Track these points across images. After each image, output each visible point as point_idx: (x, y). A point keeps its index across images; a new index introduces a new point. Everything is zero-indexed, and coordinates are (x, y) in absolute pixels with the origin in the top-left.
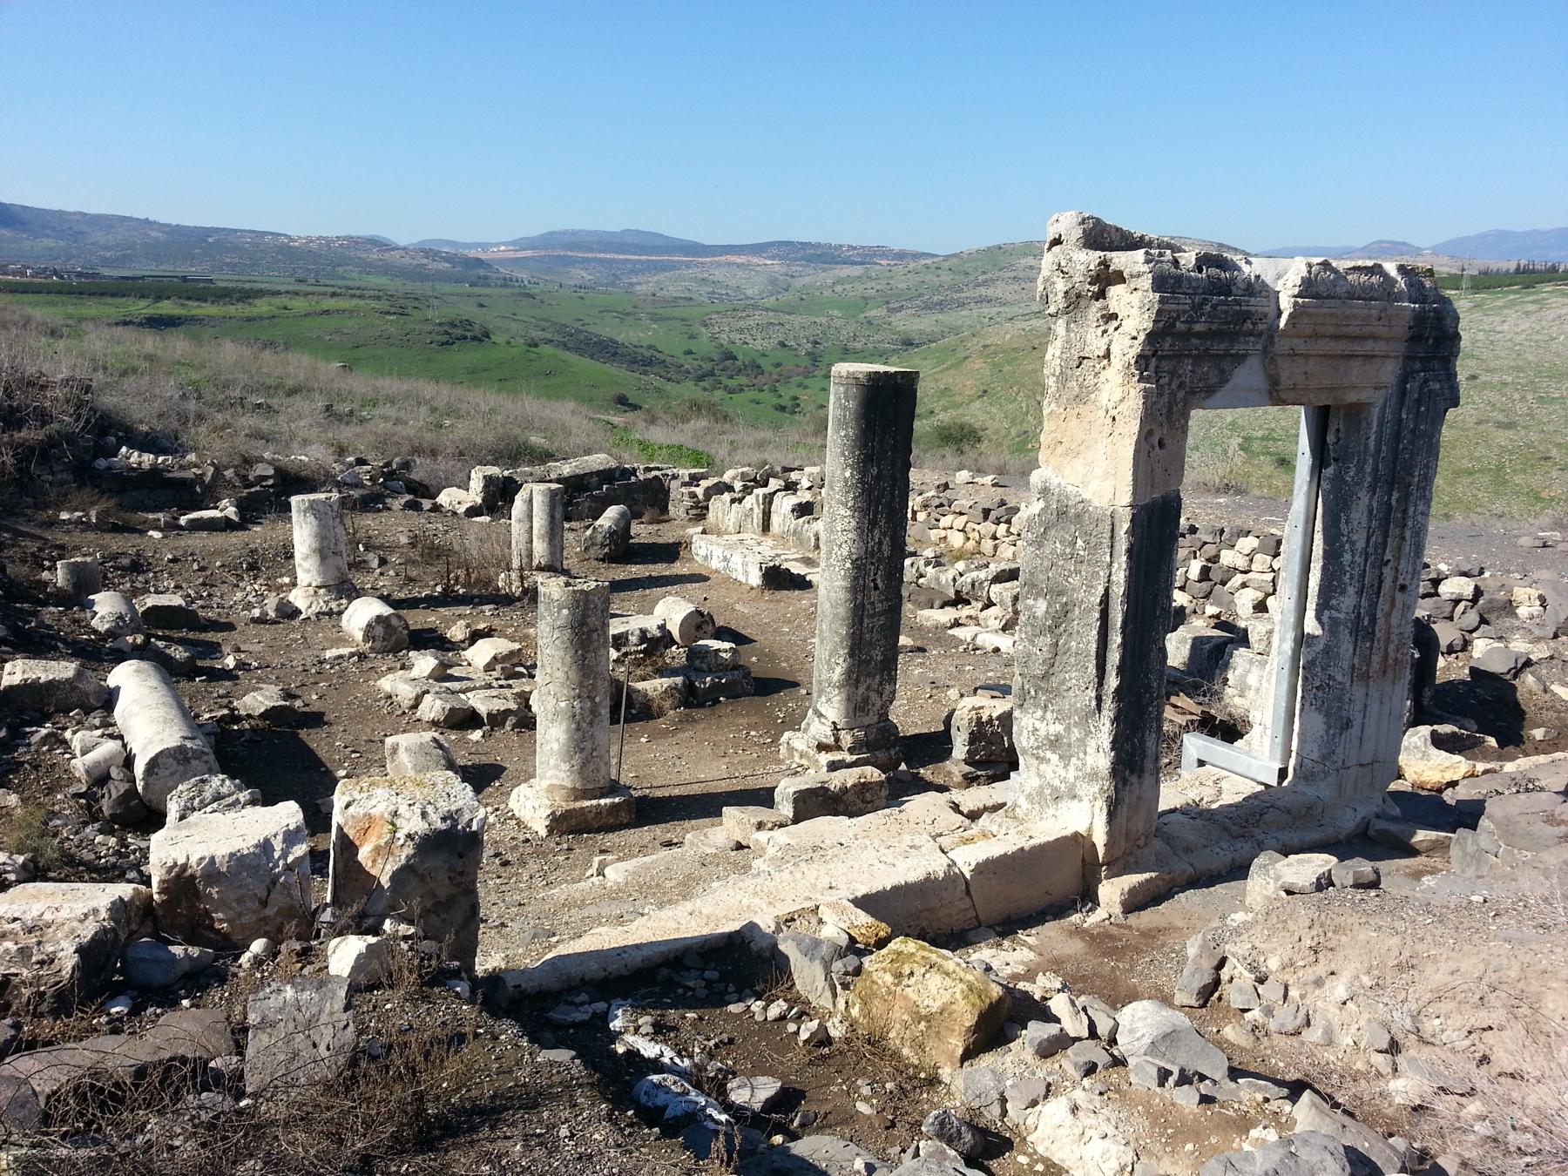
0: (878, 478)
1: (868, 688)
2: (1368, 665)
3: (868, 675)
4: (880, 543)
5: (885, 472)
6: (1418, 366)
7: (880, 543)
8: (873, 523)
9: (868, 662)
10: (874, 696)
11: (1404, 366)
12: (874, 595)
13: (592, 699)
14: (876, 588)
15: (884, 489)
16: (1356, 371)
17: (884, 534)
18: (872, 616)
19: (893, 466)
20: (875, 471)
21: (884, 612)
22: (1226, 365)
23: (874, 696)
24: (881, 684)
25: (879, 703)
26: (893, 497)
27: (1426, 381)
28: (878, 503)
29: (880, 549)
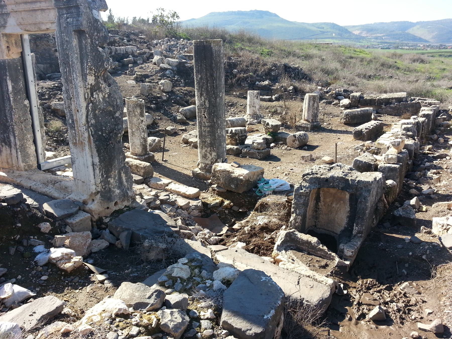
0: (201, 78)
1: (206, 151)
2: (76, 140)
3: (205, 146)
4: (205, 102)
5: (203, 77)
6: (65, 12)
7: (205, 102)
8: (201, 95)
9: (205, 142)
10: (208, 155)
11: (59, 12)
12: (204, 120)
13: (132, 130)
14: (205, 117)
15: (204, 83)
16: (39, 17)
17: (206, 99)
18: (205, 127)
19: (206, 75)
20: (200, 76)
21: (209, 126)
22: (5, 17)
23: (208, 155)
24: (210, 151)
25: (210, 158)
26: (208, 86)
27: (68, 18)
28: (202, 88)
29: (205, 104)
